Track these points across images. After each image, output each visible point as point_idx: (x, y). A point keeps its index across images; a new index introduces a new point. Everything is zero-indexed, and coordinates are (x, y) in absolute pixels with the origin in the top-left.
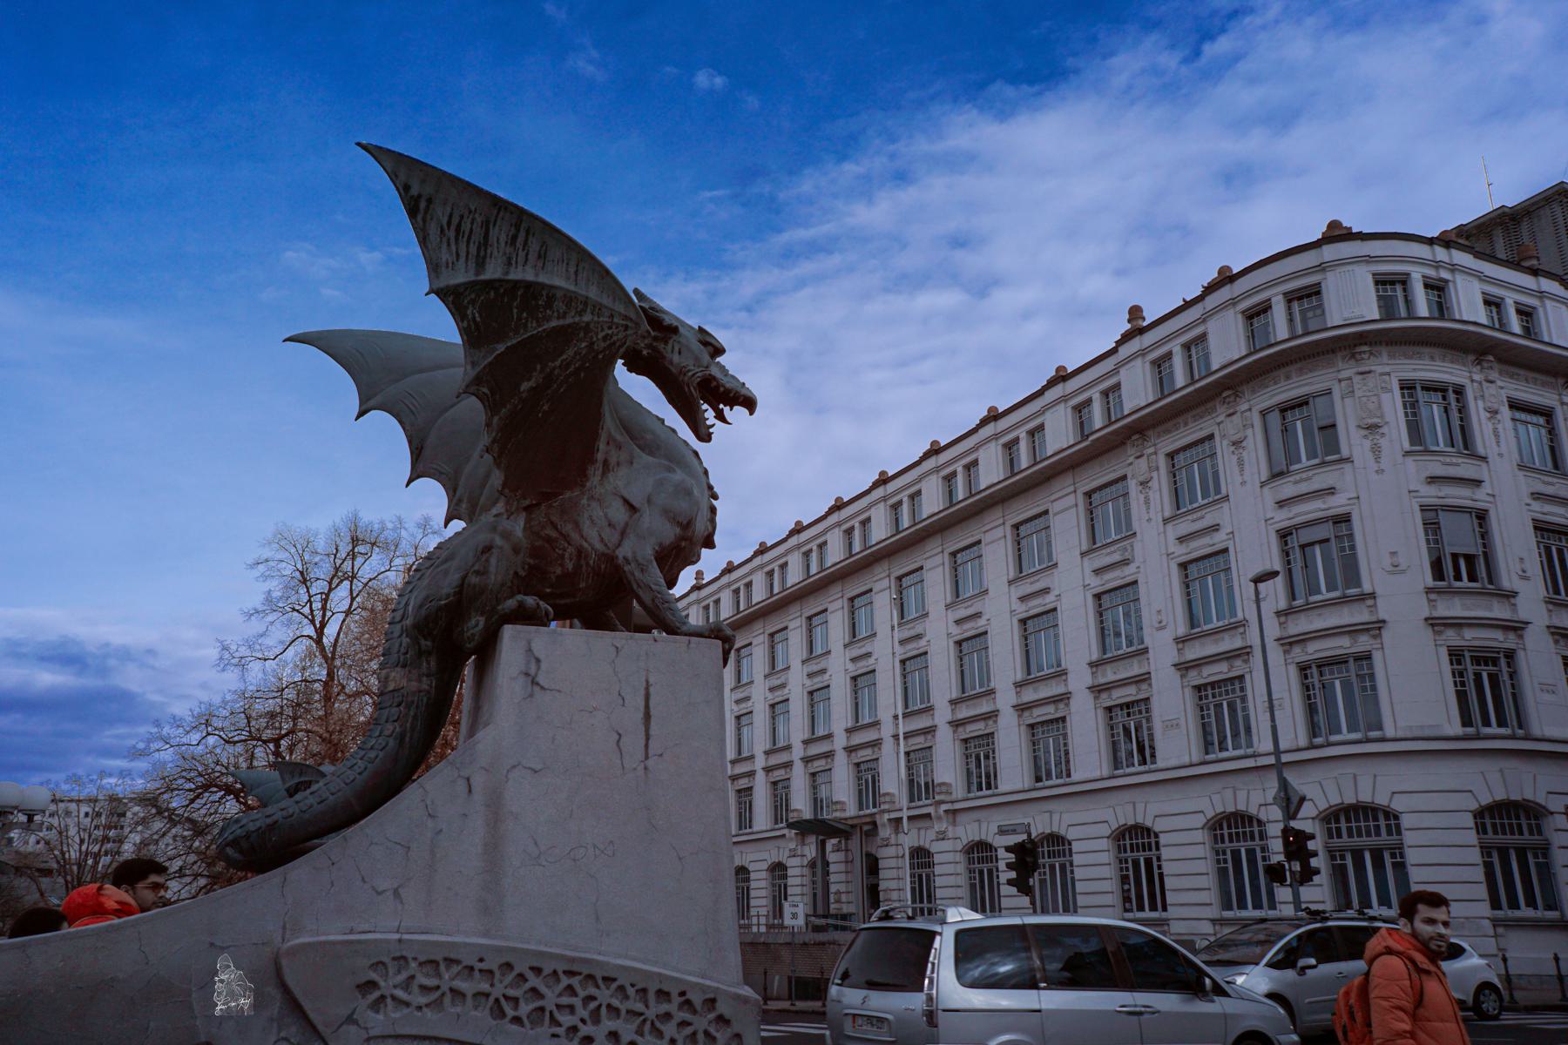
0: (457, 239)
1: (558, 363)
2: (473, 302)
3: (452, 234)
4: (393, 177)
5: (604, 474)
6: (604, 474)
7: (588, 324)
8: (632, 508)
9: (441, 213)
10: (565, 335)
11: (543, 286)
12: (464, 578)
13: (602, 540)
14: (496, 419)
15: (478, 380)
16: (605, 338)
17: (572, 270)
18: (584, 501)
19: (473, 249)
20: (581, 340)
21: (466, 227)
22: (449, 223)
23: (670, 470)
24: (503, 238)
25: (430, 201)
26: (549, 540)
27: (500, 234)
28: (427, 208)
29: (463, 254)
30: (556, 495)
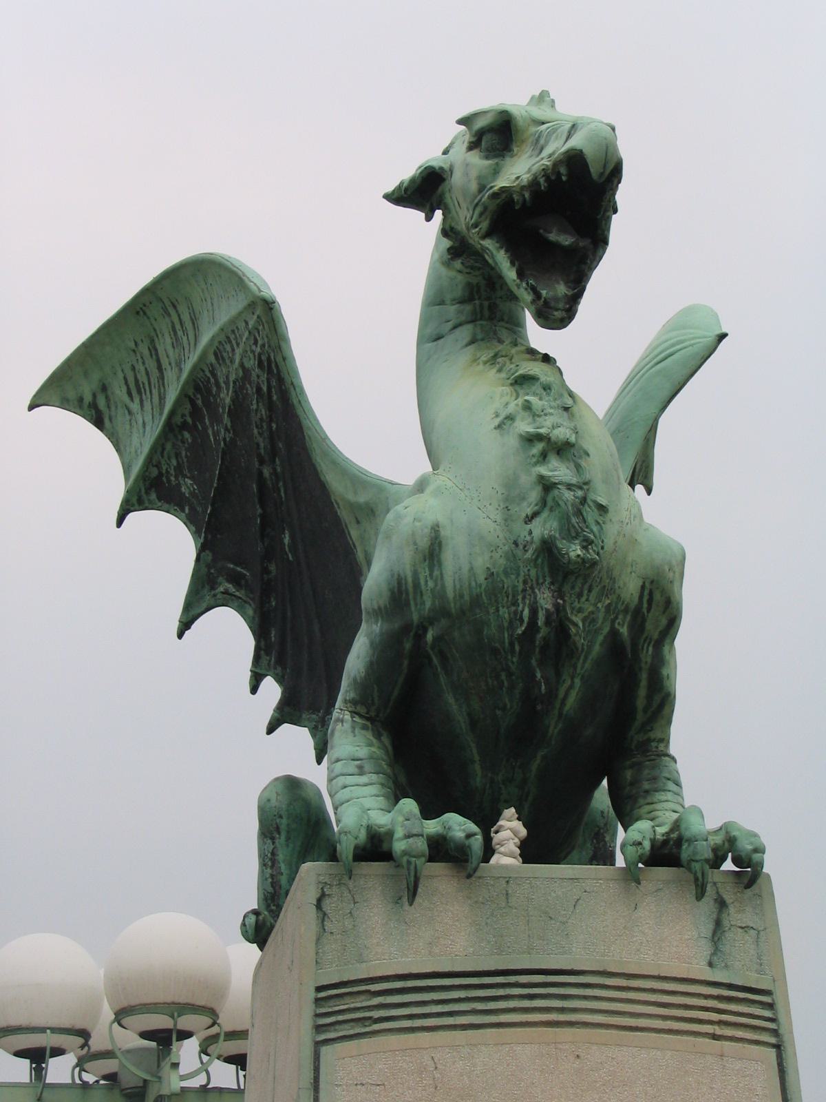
0: (141, 401)
2: (179, 469)
3: (135, 406)
4: (65, 404)
7: (242, 365)
9: (119, 392)
21: (142, 378)
22: (130, 394)
24: (168, 341)
25: (104, 388)
27: (165, 344)
28: (107, 398)
29: (148, 418)
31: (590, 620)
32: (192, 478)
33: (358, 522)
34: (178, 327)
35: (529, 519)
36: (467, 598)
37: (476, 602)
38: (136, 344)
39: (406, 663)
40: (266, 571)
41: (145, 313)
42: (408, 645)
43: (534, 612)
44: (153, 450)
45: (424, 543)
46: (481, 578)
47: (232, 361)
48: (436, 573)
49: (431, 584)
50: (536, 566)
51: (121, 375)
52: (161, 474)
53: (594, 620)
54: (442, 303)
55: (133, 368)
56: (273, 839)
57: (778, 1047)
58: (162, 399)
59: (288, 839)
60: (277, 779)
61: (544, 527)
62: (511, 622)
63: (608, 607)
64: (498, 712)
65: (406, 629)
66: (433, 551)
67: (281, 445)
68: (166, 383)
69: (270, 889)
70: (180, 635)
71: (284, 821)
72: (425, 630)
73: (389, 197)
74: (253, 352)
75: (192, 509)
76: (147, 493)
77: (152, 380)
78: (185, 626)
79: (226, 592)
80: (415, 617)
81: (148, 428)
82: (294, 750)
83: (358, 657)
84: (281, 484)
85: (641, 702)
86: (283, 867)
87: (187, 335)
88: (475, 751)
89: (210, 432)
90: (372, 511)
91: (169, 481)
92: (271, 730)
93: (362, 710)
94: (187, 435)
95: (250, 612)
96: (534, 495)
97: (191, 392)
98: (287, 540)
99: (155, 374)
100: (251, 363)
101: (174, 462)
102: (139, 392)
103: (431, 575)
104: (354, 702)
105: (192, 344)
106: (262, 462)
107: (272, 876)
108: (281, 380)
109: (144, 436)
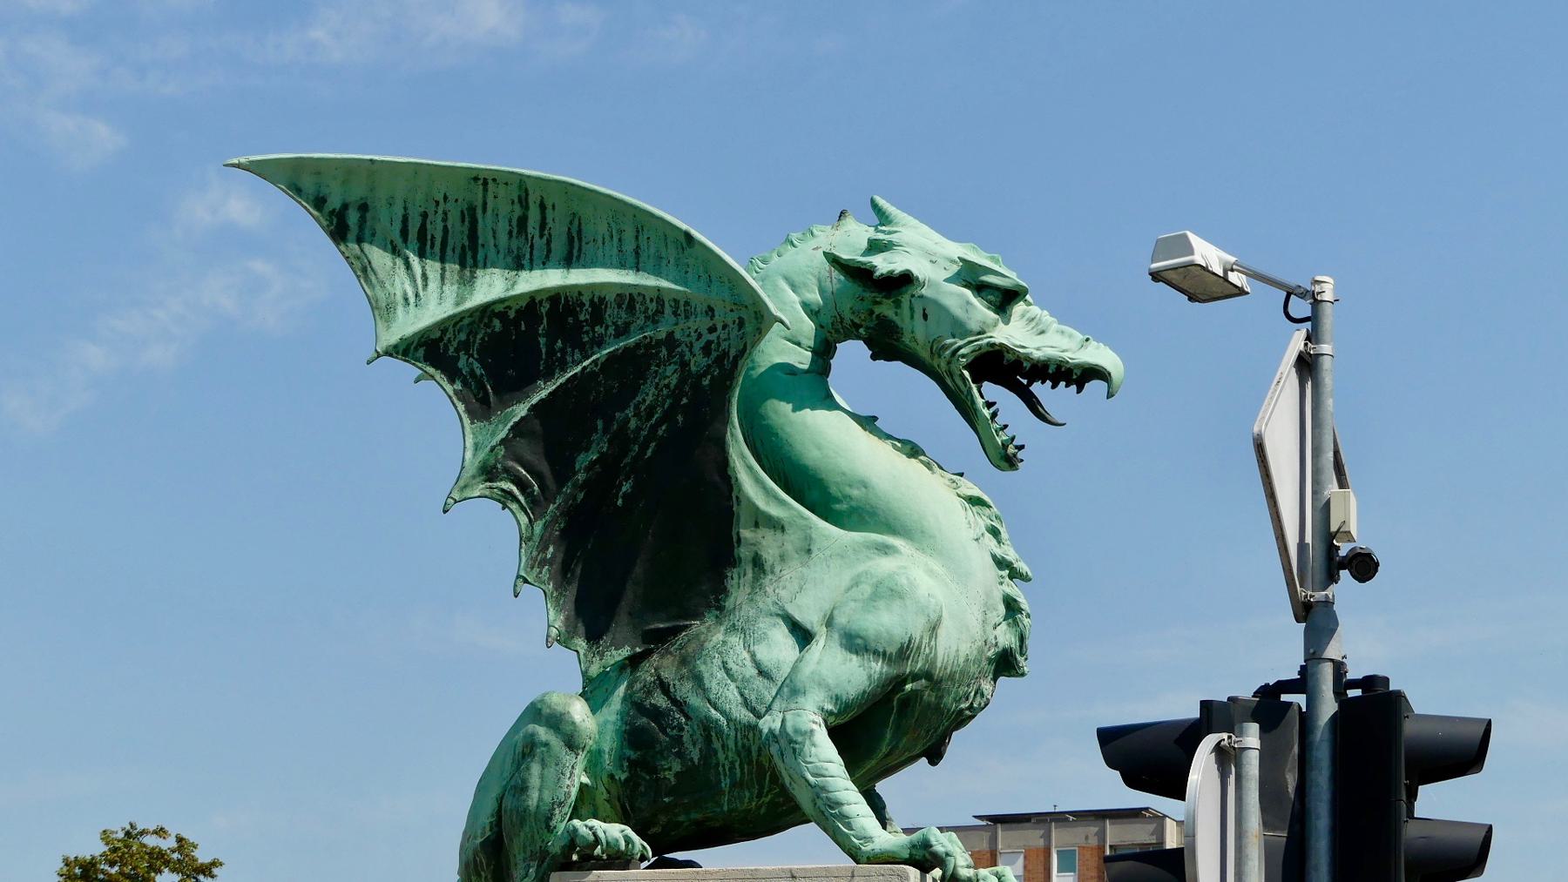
1: (630, 412)
2: (465, 346)
4: (296, 190)
5: (756, 579)
6: (756, 579)
7: (670, 335)
8: (803, 636)
9: (387, 220)
10: (632, 366)
11: (579, 290)
12: (500, 800)
13: (746, 703)
14: (538, 527)
15: (489, 473)
16: (706, 349)
17: (629, 246)
18: (719, 637)
20: (668, 362)
22: (404, 233)
23: (885, 550)
24: (503, 228)
25: (364, 208)
26: (656, 714)
28: (362, 220)
30: (675, 631)
32: (484, 366)
37: (951, 677)
38: (445, 198)
41: (485, 183)
44: (454, 316)
45: (934, 617)
46: (961, 660)
47: (654, 318)
51: (400, 212)
52: (441, 339)
54: (799, 344)
55: (425, 215)
61: (1005, 637)
65: (898, 676)
66: (933, 629)
67: (680, 418)
68: (480, 257)
72: (904, 682)
74: (700, 336)
76: (416, 349)
77: (451, 242)
79: (509, 494)
81: (433, 285)
87: (549, 242)
89: (542, 340)
90: (783, 529)
91: (446, 348)
94: (497, 324)
96: (1002, 609)
98: (626, 487)
104: (831, 713)
109: (425, 286)
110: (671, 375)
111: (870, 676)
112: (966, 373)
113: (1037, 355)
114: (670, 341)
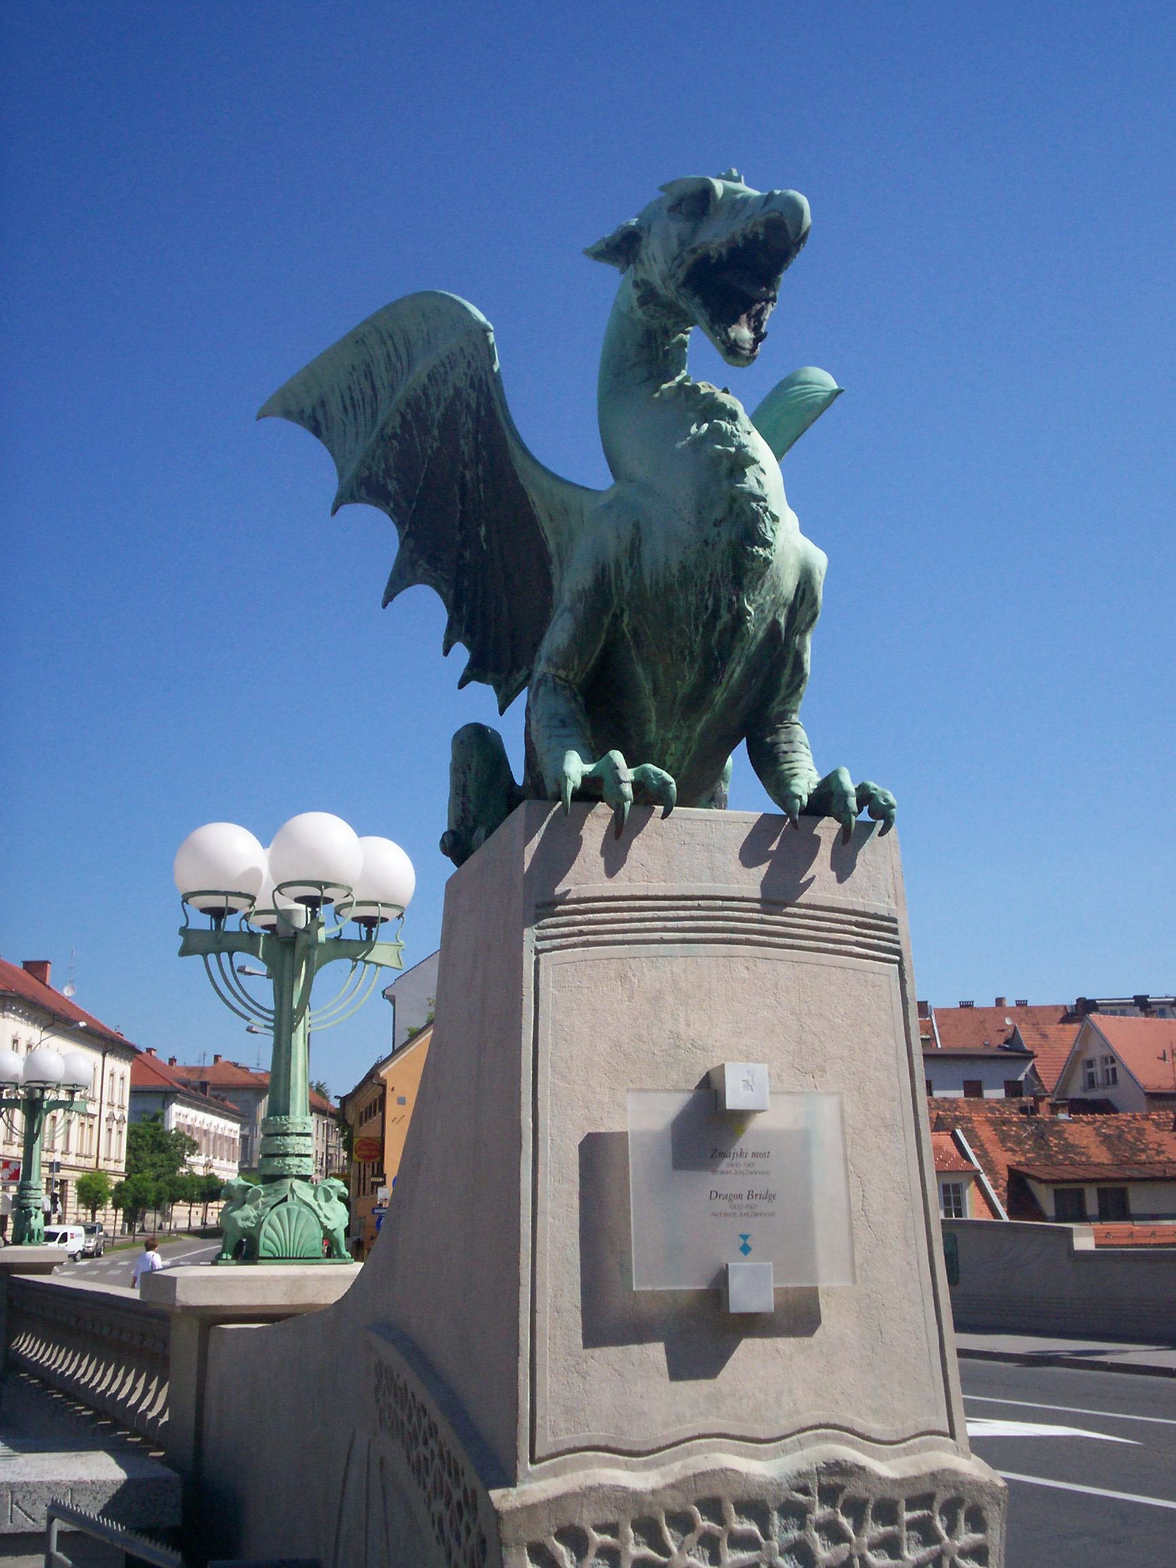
0: (356, 419)
2: (387, 471)
4: (288, 414)
16: (472, 385)
19: (369, 411)
21: (357, 396)
24: (383, 366)
25: (323, 404)
28: (325, 413)
31: (760, 609)
32: (398, 480)
33: (552, 520)
34: (393, 354)
35: (717, 524)
36: (661, 585)
38: (353, 367)
39: (603, 637)
40: (462, 557)
41: (364, 342)
42: (607, 620)
43: (717, 600)
46: (675, 568)
47: (445, 382)
48: (635, 563)
49: (631, 571)
50: (722, 562)
53: (762, 611)
55: (350, 388)
56: (464, 773)
57: (900, 963)
58: (374, 415)
59: (476, 774)
60: (467, 726)
62: (698, 608)
63: (773, 601)
64: (679, 682)
69: (461, 814)
70: (385, 605)
71: (474, 760)
73: (586, 252)
74: (466, 374)
75: (397, 504)
78: (388, 598)
80: (616, 600)
82: (480, 703)
83: (559, 633)
84: (481, 486)
85: (785, 679)
86: (473, 796)
88: (653, 711)
91: (378, 481)
92: (462, 685)
93: (562, 673)
94: (395, 443)
95: (445, 590)
97: (402, 407)
98: (483, 531)
99: (369, 392)
100: (462, 384)
101: (383, 466)
102: (354, 406)
103: (631, 564)
105: (406, 367)
106: (465, 467)
107: (463, 803)
108: (490, 399)
110: (467, 423)
111: (575, 619)
112: (682, 290)
113: (724, 240)
114: (457, 391)
